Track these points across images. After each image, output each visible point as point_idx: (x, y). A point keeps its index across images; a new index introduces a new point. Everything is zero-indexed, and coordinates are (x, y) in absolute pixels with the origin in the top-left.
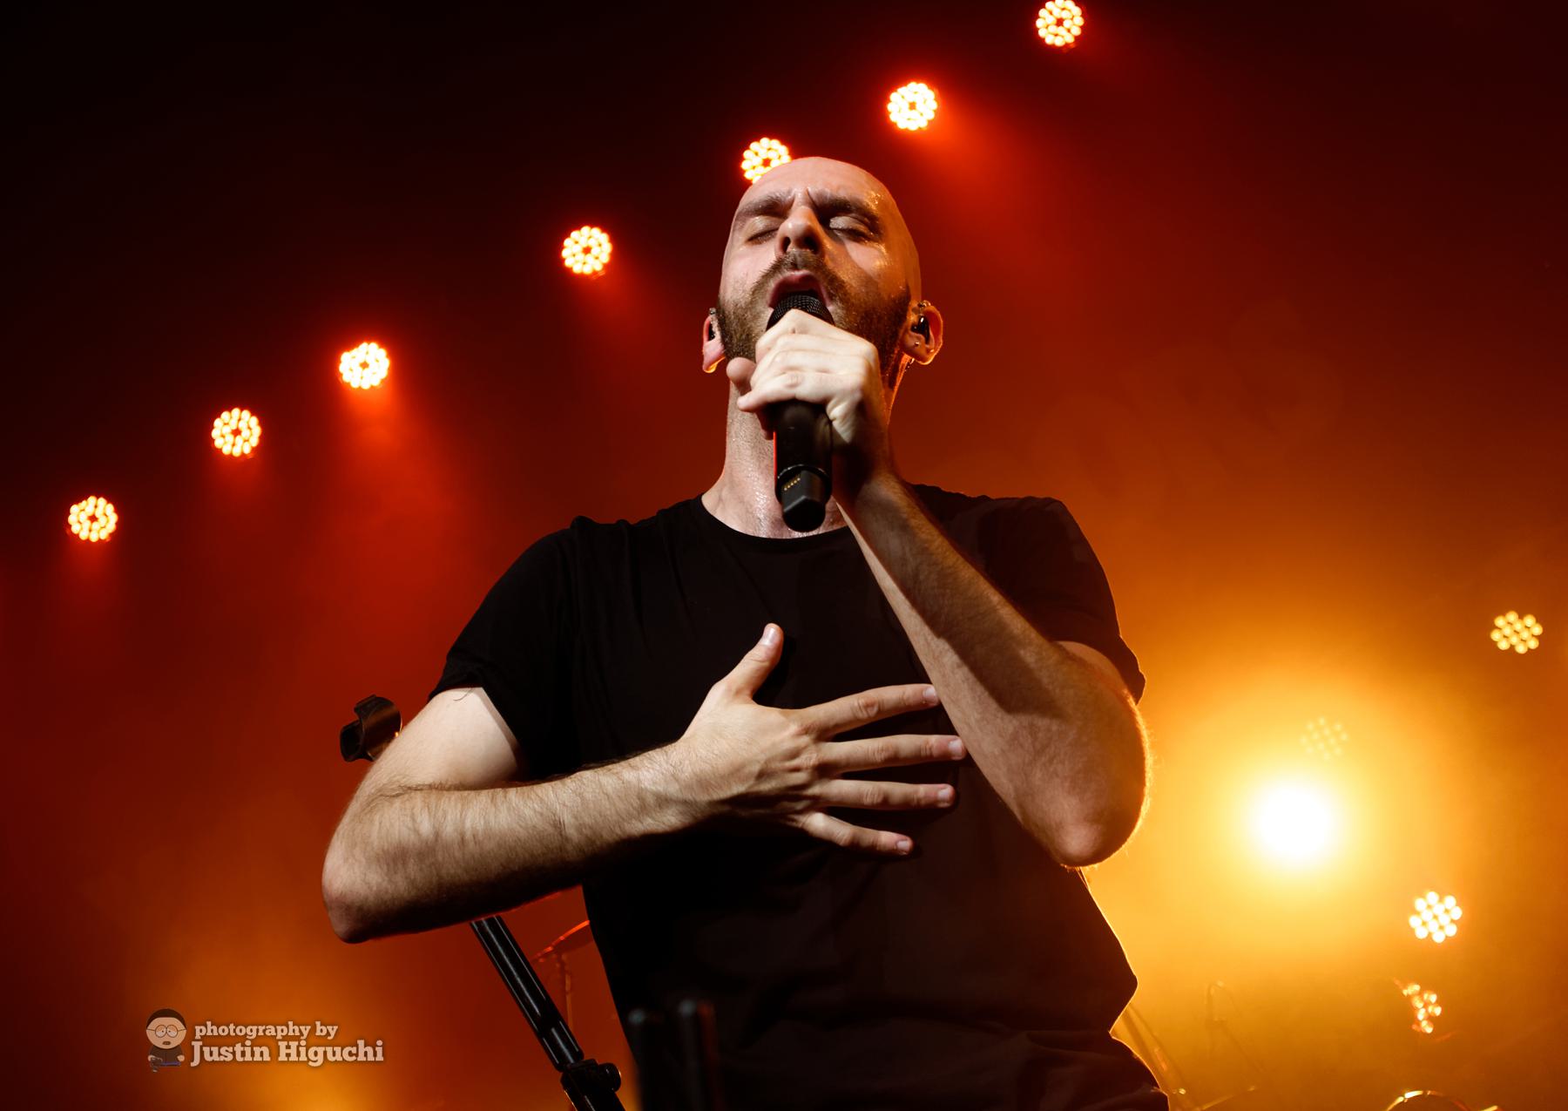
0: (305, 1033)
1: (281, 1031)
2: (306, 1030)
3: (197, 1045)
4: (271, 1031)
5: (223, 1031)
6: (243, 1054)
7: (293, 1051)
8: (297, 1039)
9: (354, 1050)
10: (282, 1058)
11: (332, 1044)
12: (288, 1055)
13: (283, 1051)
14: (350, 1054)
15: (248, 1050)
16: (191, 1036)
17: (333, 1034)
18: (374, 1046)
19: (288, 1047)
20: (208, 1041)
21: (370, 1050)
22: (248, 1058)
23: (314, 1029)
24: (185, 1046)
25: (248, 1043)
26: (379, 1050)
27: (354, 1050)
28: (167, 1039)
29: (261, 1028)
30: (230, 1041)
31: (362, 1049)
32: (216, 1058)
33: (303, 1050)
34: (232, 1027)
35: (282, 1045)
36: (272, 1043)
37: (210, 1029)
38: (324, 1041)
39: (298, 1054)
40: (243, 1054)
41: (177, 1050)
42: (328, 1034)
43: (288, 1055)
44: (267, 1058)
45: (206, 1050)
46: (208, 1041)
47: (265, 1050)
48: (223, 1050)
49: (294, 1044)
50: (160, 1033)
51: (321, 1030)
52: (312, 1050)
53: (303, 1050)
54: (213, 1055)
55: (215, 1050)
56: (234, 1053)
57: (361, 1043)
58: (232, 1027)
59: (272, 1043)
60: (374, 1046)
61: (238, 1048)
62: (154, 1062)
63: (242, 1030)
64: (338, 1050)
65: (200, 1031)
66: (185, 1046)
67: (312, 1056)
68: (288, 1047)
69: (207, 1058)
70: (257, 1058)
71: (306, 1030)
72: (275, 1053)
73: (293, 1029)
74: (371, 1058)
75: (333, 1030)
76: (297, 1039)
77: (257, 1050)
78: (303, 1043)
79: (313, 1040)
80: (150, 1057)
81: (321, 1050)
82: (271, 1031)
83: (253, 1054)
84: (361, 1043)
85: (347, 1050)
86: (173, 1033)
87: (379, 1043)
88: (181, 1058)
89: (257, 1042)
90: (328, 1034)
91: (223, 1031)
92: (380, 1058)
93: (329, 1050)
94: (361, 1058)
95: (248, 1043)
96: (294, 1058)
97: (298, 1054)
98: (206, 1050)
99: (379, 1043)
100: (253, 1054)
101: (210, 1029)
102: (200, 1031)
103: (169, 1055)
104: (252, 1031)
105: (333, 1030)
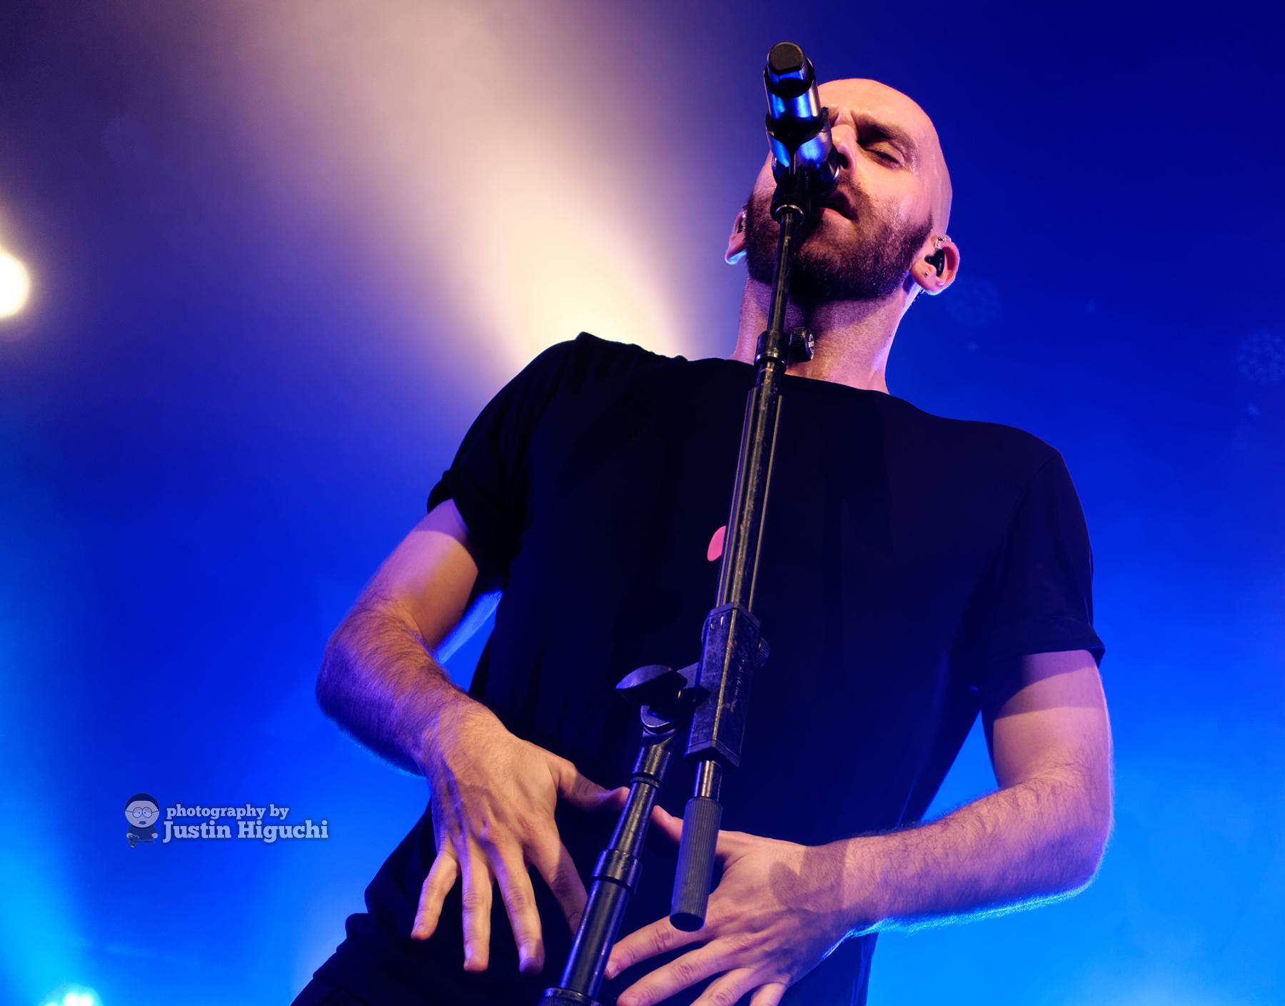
0: (261, 814)
1: (240, 812)
2: (261, 812)
3: (168, 824)
4: (231, 812)
5: (191, 812)
6: (208, 832)
7: (251, 829)
8: (254, 819)
9: (303, 829)
10: (241, 835)
11: (284, 823)
12: (246, 833)
14: (300, 832)
15: (212, 829)
16: (163, 817)
17: (284, 814)
18: (320, 826)
19: (246, 826)
20: (178, 821)
21: (316, 828)
22: (212, 835)
23: (268, 811)
24: (159, 826)
25: (212, 823)
26: (324, 829)
27: (303, 829)
28: (142, 819)
29: (223, 810)
30: (197, 821)
31: (309, 828)
32: (184, 835)
33: (259, 829)
34: (198, 809)
35: (242, 824)
36: (232, 823)
37: (180, 811)
38: (276, 821)
39: (255, 832)
40: (208, 832)
41: (151, 829)
42: (281, 815)
43: (246, 833)
44: (228, 835)
45: (176, 828)
46: (178, 821)
47: (227, 828)
48: (191, 828)
49: (251, 824)
50: (136, 814)
51: (274, 812)
52: (267, 829)
53: (259, 829)
54: (183, 833)
55: (184, 828)
56: (200, 831)
57: (309, 822)
58: (198, 809)
59: (232, 823)
60: (320, 826)
61: (204, 827)
62: (131, 839)
63: (206, 812)
64: (289, 828)
65: (171, 812)
66: (159, 826)
68: (246, 826)
70: (220, 835)
71: (261, 812)
72: (235, 831)
73: (250, 811)
74: (317, 835)
76: (254, 819)
77: (220, 829)
78: (259, 823)
79: (268, 821)
80: (128, 835)
81: (274, 829)
82: (231, 812)
84: (309, 822)
86: (148, 814)
88: (155, 836)
89: (221, 821)
90: (281, 815)
91: (191, 812)
92: (325, 835)
93: (282, 828)
94: (309, 835)
95: (212, 823)
96: (251, 835)
97: (255, 832)
98: (176, 828)
99: (324, 822)
101: (180, 811)
102: (171, 812)
103: (144, 833)
104: (215, 813)
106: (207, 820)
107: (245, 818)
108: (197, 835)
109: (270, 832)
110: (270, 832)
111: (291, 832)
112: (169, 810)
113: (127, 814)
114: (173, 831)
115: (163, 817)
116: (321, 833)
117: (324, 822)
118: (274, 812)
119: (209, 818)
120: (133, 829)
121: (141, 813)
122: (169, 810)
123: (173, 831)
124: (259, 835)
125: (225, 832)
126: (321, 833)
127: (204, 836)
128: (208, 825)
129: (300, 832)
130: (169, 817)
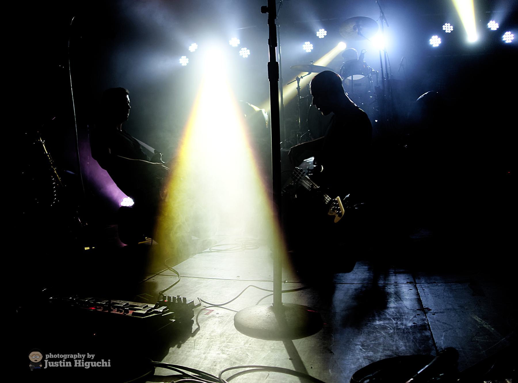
0: (84, 357)
2: (84, 356)
3: (46, 361)
4: (72, 356)
5: (55, 356)
6: (62, 364)
7: (79, 363)
9: (100, 363)
10: (76, 366)
11: (93, 361)
12: (78, 365)
13: (76, 363)
14: (99, 364)
15: (64, 363)
16: (44, 358)
17: (93, 357)
18: (107, 362)
19: (78, 362)
20: (50, 360)
21: (106, 363)
22: (64, 366)
23: (86, 356)
24: (43, 362)
25: (64, 360)
26: (109, 363)
28: (36, 359)
29: (68, 355)
30: (58, 360)
31: (103, 363)
32: (53, 366)
33: (83, 363)
34: (58, 355)
35: (76, 361)
36: (72, 361)
37: (51, 356)
38: (90, 360)
39: (81, 364)
40: (62, 364)
42: (92, 357)
43: (78, 365)
44: (70, 366)
46: (50, 360)
47: (70, 363)
49: (80, 361)
50: (33, 357)
51: (89, 356)
52: (86, 363)
53: (83, 363)
54: (52, 365)
55: (52, 363)
56: (59, 364)
57: (103, 360)
58: (58, 355)
59: (72, 361)
60: (107, 362)
61: (61, 362)
62: (31, 367)
63: (62, 356)
64: (95, 363)
65: (47, 356)
66: (43, 362)
68: (78, 362)
69: (50, 366)
70: (67, 366)
71: (84, 356)
72: (73, 363)
73: (79, 356)
74: (106, 366)
75: (93, 356)
77: (67, 363)
78: (83, 360)
79: (86, 360)
80: (30, 365)
81: (89, 363)
82: (72, 356)
83: (66, 364)
84: (103, 360)
85: (98, 363)
86: (38, 357)
87: (109, 360)
89: (67, 360)
90: (92, 357)
91: (55, 356)
92: (109, 366)
93: (92, 363)
94: (103, 366)
95: (64, 360)
96: (80, 366)
97: (81, 364)
98: (49, 363)
100: (66, 364)
101: (51, 356)
102: (47, 356)
104: (65, 356)
105: (93, 356)
107: (77, 359)
108: (58, 366)
109: (87, 364)
110: (87, 364)
112: (46, 355)
113: (30, 357)
115: (44, 358)
116: (108, 364)
117: (109, 360)
118: (89, 356)
121: (35, 357)
122: (46, 355)
124: (83, 366)
125: (69, 364)
126: (108, 364)
127: (61, 366)
128: (62, 361)
129: (99, 364)
130: (47, 358)
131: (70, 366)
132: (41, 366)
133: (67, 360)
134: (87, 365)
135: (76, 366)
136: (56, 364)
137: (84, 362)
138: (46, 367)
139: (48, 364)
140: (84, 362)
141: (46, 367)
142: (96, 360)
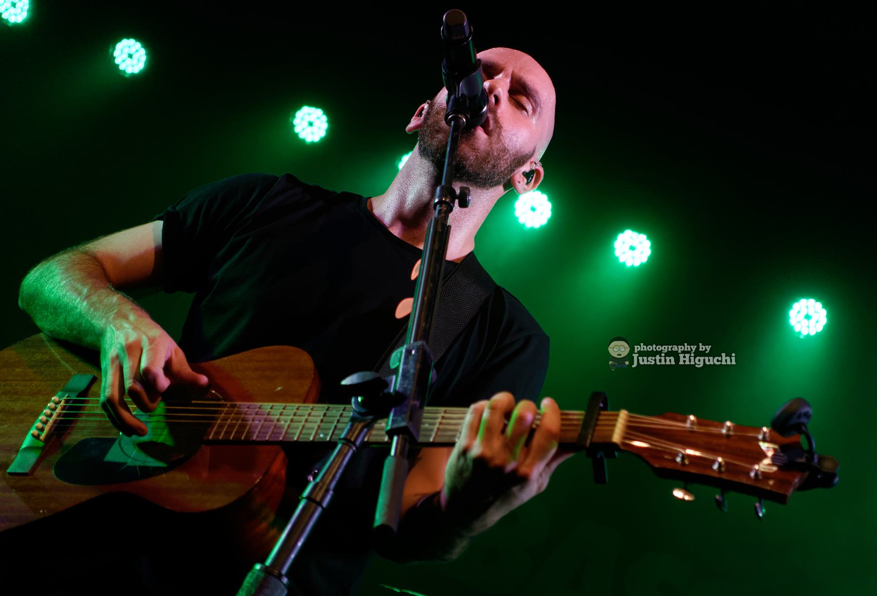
0: (694, 350)
1: (680, 348)
2: (694, 348)
3: (635, 356)
4: (675, 348)
5: (650, 348)
6: (660, 361)
7: (687, 359)
8: (689, 352)
9: (720, 359)
10: (681, 363)
11: (708, 355)
13: (682, 359)
14: (718, 361)
15: (663, 359)
16: (632, 351)
17: (708, 350)
20: (641, 354)
21: (728, 358)
22: (663, 363)
23: (698, 348)
24: (630, 357)
26: (733, 359)
27: (720, 359)
30: (653, 354)
33: (692, 359)
34: (654, 346)
35: (681, 356)
36: (676, 355)
37: (643, 347)
38: (703, 354)
39: (690, 361)
40: (660, 361)
41: (625, 359)
44: (673, 363)
45: (640, 358)
46: (641, 354)
47: (672, 358)
48: (650, 358)
49: (687, 355)
50: (615, 350)
51: (702, 348)
52: (697, 358)
53: (692, 359)
55: (645, 358)
56: (655, 360)
57: (723, 355)
58: (654, 346)
59: (676, 355)
60: (731, 356)
61: (658, 357)
62: (612, 365)
63: (659, 348)
64: (711, 358)
65: (637, 348)
66: (630, 357)
67: (697, 362)
69: (641, 363)
70: (668, 363)
71: (694, 348)
72: (677, 360)
73: (687, 347)
74: (729, 363)
75: (708, 348)
76: (689, 352)
79: (698, 353)
80: (610, 363)
81: (702, 358)
82: (675, 348)
84: (723, 355)
85: (716, 358)
86: (623, 349)
88: (627, 363)
89: (668, 354)
91: (650, 348)
92: (734, 363)
93: (706, 358)
94: (724, 363)
96: (687, 363)
97: (690, 361)
98: (640, 358)
99: (733, 355)
101: (643, 347)
102: (637, 348)
103: (621, 361)
104: (665, 349)
105: (708, 348)
106: (660, 353)
107: (684, 352)
108: (653, 363)
111: (712, 361)
113: (610, 350)
114: (638, 360)
115: (632, 351)
117: (733, 355)
118: (702, 348)
119: (661, 352)
120: (614, 359)
123: (638, 360)
124: (692, 363)
127: (658, 363)
129: (718, 361)
130: (636, 351)
131: (673, 363)
132: (627, 363)
133: (668, 354)
134: (700, 362)
135: (681, 363)
136: (651, 361)
137: (695, 357)
138: (635, 365)
139: (638, 361)
140: (695, 357)
141: (635, 365)
142: (712, 354)
